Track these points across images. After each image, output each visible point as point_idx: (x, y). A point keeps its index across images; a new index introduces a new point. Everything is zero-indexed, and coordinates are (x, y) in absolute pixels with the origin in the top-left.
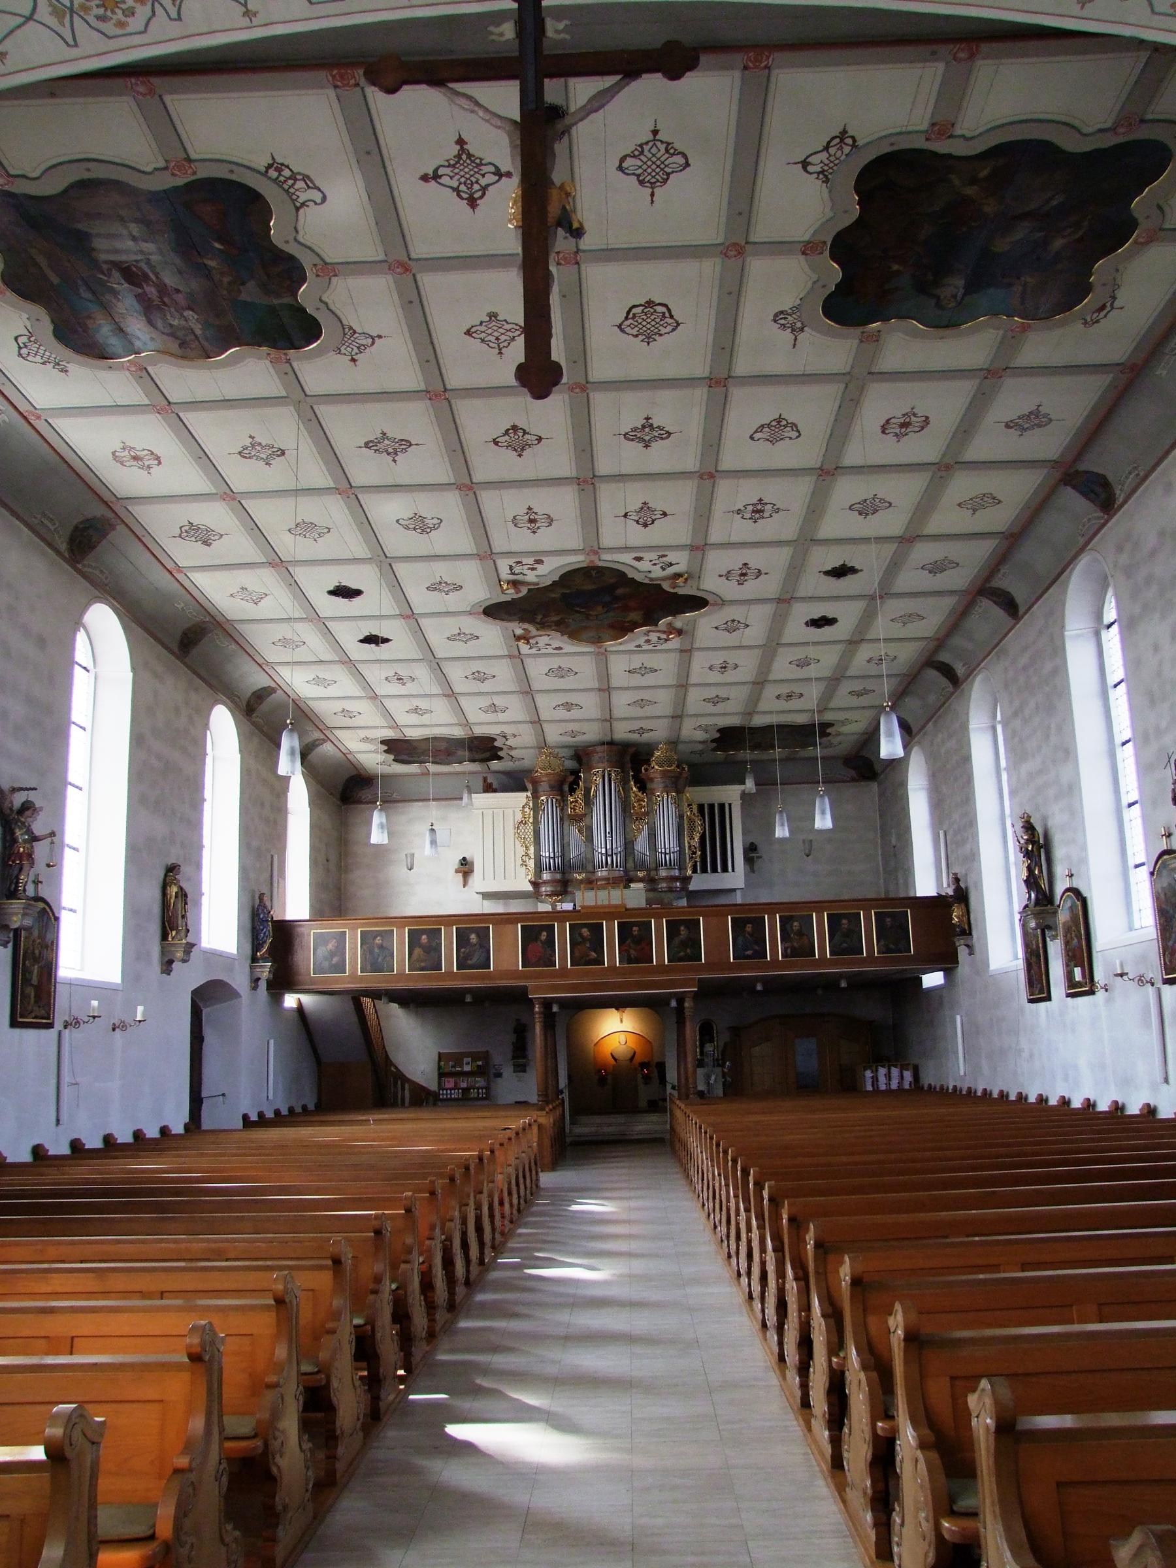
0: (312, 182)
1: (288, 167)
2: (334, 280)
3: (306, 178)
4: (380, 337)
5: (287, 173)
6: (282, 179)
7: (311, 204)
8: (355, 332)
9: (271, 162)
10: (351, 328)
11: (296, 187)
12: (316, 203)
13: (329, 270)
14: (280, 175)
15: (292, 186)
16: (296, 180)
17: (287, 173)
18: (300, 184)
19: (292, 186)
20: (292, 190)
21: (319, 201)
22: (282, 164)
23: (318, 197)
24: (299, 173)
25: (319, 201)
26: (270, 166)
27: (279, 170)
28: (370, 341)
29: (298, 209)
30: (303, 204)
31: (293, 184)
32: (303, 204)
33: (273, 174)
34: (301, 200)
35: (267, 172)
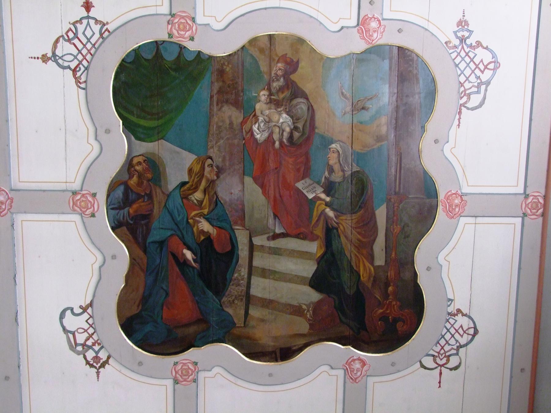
0: (68, 338)
1: (88, 363)
2: (76, 186)
3: (73, 346)
4: (45, 59)
5: (90, 354)
6: (97, 348)
7: (78, 310)
8: (74, 71)
9: (101, 370)
10: (78, 81)
11: (86, 335)
12: (72, 309)
13: (78, 201)
14: (97, 353)
15: (91, 336)
16: (84, 345)
17: (90, 354)
18: (81, 338)
19: (91, 336)
20: (91, 331)
21: (68, 312)
22: (92, 366)
23: (69, 319)
24: (78, 353)
25: (68, 312)
26: (103, 366)
27: (96, 358)
28: (59, 52)
29: (91, 305)
30: (84, 310)
31: (87, 339)
32: (84, 310)
33: (103, 355)
34: (86, 316)
35: (109, 357)
